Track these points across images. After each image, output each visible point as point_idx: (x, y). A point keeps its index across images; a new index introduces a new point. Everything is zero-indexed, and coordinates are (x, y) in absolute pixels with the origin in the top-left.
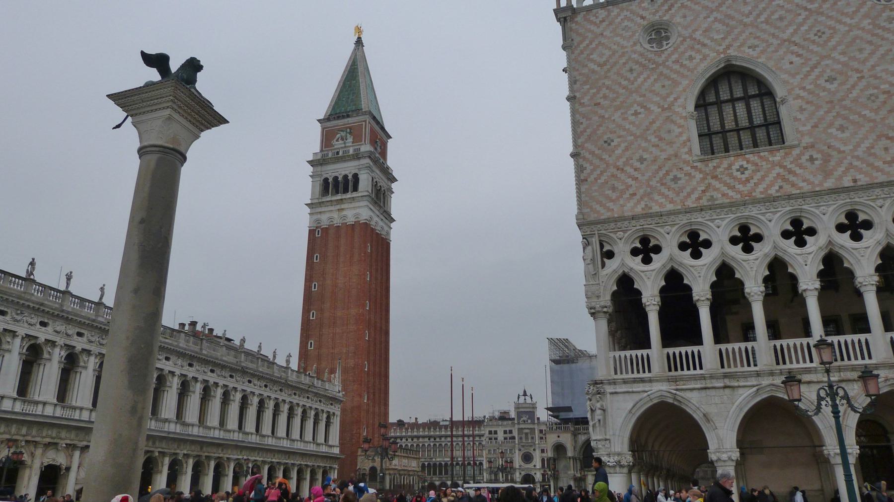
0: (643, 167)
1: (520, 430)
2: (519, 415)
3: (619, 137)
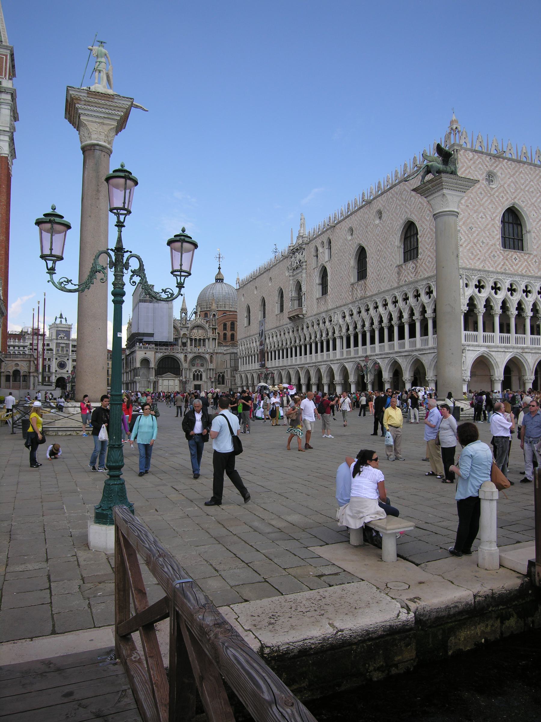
0: (483, 246)
1: (58, 344)
2: (58, 333)
3: (475, 227)
